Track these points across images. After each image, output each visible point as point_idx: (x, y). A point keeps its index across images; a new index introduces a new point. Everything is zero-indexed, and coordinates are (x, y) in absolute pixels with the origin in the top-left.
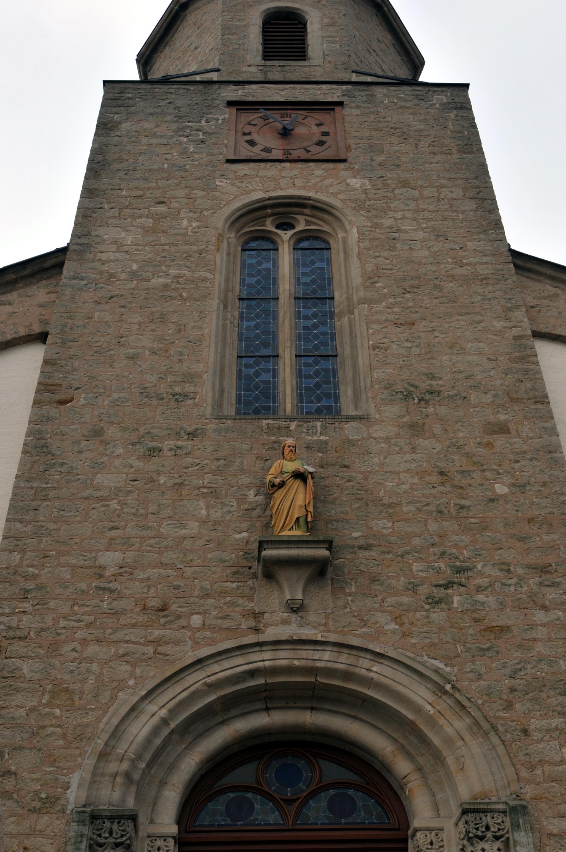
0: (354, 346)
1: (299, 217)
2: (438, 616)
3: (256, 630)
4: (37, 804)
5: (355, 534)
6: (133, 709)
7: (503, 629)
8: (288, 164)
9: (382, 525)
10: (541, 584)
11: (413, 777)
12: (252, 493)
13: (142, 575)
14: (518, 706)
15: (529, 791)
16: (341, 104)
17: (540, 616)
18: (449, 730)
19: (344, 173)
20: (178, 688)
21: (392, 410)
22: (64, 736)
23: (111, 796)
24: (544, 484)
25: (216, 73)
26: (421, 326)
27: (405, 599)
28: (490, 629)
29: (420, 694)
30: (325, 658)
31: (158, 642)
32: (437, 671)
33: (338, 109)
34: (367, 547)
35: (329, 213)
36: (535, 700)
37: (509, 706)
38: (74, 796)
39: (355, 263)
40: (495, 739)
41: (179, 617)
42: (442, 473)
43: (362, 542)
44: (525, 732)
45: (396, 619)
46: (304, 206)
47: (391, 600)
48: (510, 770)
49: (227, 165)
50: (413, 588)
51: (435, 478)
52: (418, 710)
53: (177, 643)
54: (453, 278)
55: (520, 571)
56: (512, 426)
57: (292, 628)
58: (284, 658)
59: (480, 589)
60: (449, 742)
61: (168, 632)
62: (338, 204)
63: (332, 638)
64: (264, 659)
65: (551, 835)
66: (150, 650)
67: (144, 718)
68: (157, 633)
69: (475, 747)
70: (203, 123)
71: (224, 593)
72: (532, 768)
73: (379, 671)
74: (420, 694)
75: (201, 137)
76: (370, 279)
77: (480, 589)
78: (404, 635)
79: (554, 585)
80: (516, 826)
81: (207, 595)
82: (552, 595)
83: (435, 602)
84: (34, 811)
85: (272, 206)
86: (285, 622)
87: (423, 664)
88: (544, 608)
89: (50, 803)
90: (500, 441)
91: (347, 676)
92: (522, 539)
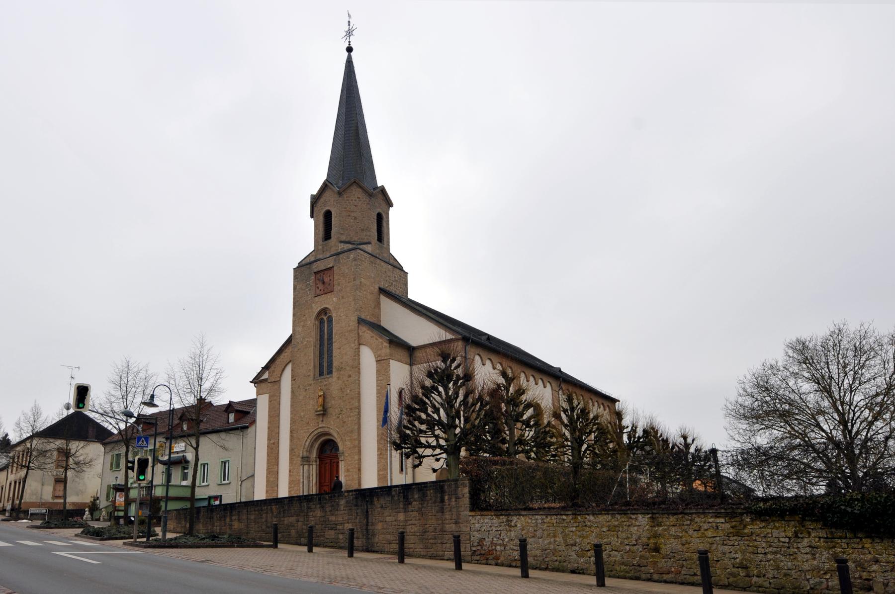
23: (305, 454)
62: (331, 308)
64: (320, 430)
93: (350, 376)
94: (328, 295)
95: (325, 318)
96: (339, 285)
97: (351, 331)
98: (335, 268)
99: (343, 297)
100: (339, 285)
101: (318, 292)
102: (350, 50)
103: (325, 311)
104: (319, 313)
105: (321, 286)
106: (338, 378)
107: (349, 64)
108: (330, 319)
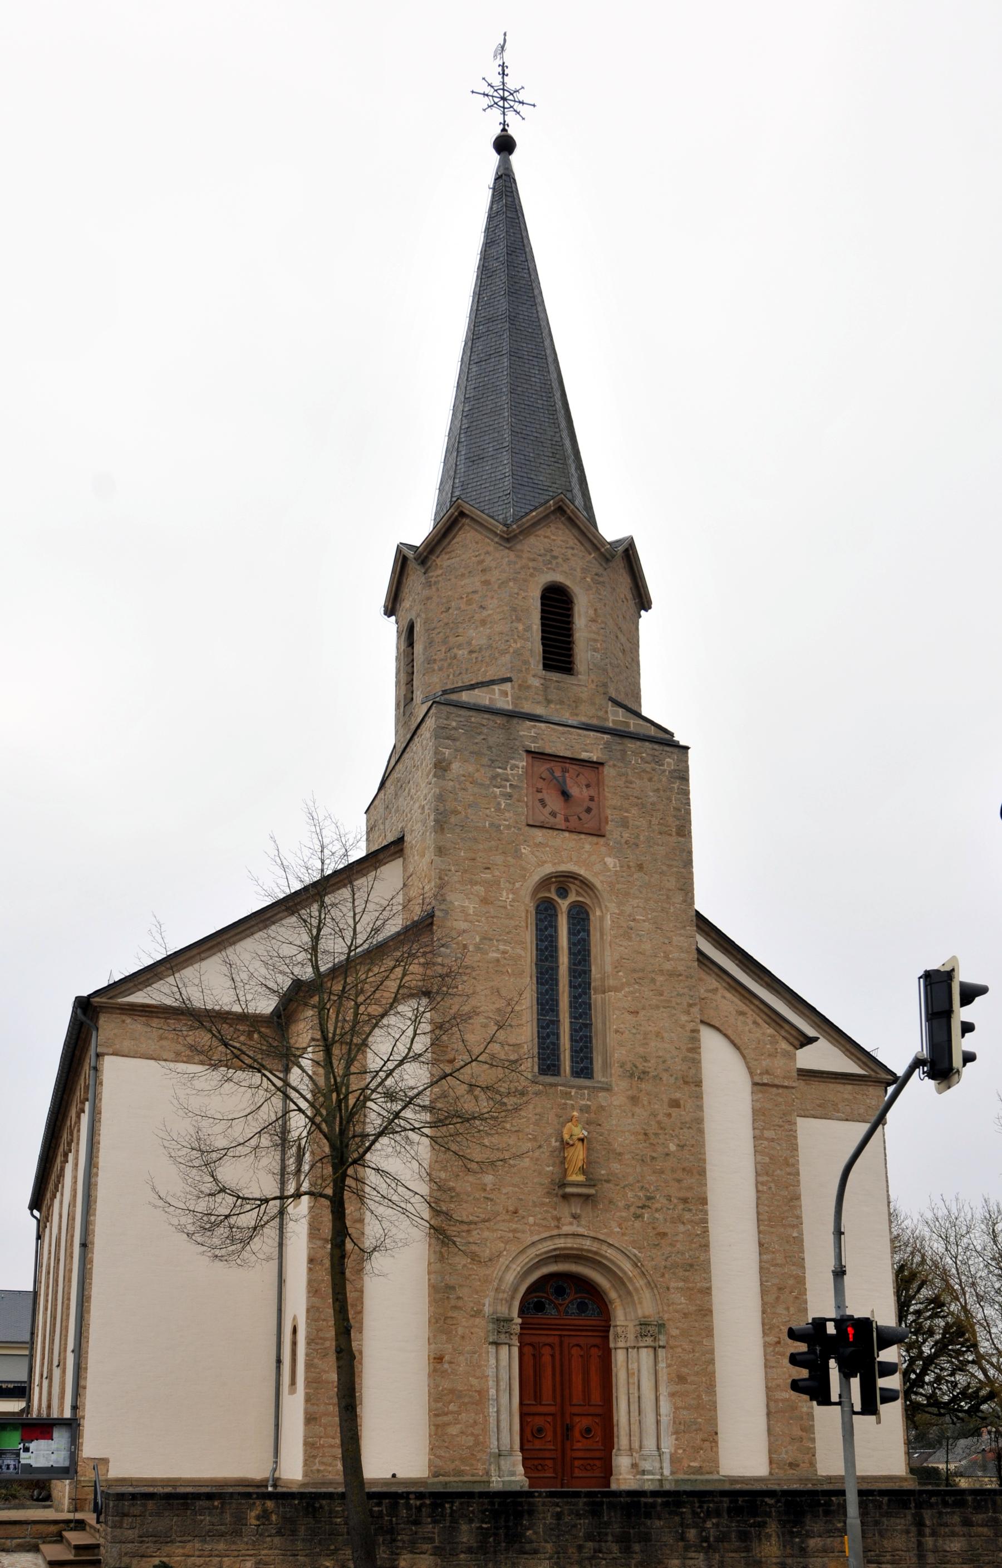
0: (604, 1023)
1: (571, 885)
2: (637, 1224)
3: (558, 1227)
4: (473, 1313)
5: (603, 1172)
6: (507, 1266)
7: (665, 1234)
8: (567, 834)
9: (616, 1167)
10: (684, 1209)
11: (618, 1300)
12: (553, 1140)
13: (504, 1191)
14: (666, 1276)
15: (666, 1316)
16: (602, 764)
17: (681, 1228)
18: (638, 1285)
19: (603, 849)
20: (524, 1256)
21: (624, 1084)
22: (480, 1280)
24: (693, 1146)
25: (509, 684)
26: (642, 1013)
27: (624, 1214)
28: (659, 1234)
29: (627, 1266)
30: (587, 1244)
31: (515, 1231)
32: (635, 1255)
33: (601, 768)
34: (608, 1181)
35: (592, 889)
36: (674, 1273)
37: (663, 1275)
38: (487, 1310)
39: (607, 953)
40: (656, 1291)
41: (523, 1218)
42: (646, 1134)
43: (605, 1178)
44: (668, 1289)
45: (620, 1226)
46: (576, 879)
47: (618, 1214)
48: (660, 1307)
49: (527, 828)
50: (627, 1207)
51: (641, 1137)
52: (625, 1273)
53: (523, 1232)
54: (661, 972)
55: (676, 1201)
56: (682, 1102)
57: (575, 1230)
58: (569, 1243)
59: (657, 1210)
60: (636, 1290)
61: (518, 1226)
62: (598, 885)
63: (592, 1234)
64: (561, 1243)
65: (672, 1336)
66: (511, 1235)
67: (511, 1271)
68: (514, 1226)
69: (647, 1295)
70: (509, 771)
71: (543, 1204)
72: (669, 1306)
73: (610, 1253)
74: (627, 1266)
75: (508, 790)
76: (618, 966)
77: (657, 1210)
78: (623, 1234)
79: (690, 1210)
80: (660, 1332)
81: (535, 1205)
82: (687, 1216)
83: (637, 1217)
84: (472, 1316)
85: (556, 877)
86: (571, 1224)
87: (629, 1251)
88: (683, 1223)
89: (478, 1313)
90: (675, 1112)
91: (596, 1253)
92: (679, 1181)
93: (675, 1104)
94: (588, 843)
95: (564, 905)
96: (625, 824)
97: (673, 974)
98: (608, 771)
99: (640, 867)
100: (625, 824)
101: (543, 815)
102: (505, 145)
103: (563, 882)
104: (545, 882)
105: (555, 802)
106: (634, 1100)
107: (505, 186)
108: (580, 917)
